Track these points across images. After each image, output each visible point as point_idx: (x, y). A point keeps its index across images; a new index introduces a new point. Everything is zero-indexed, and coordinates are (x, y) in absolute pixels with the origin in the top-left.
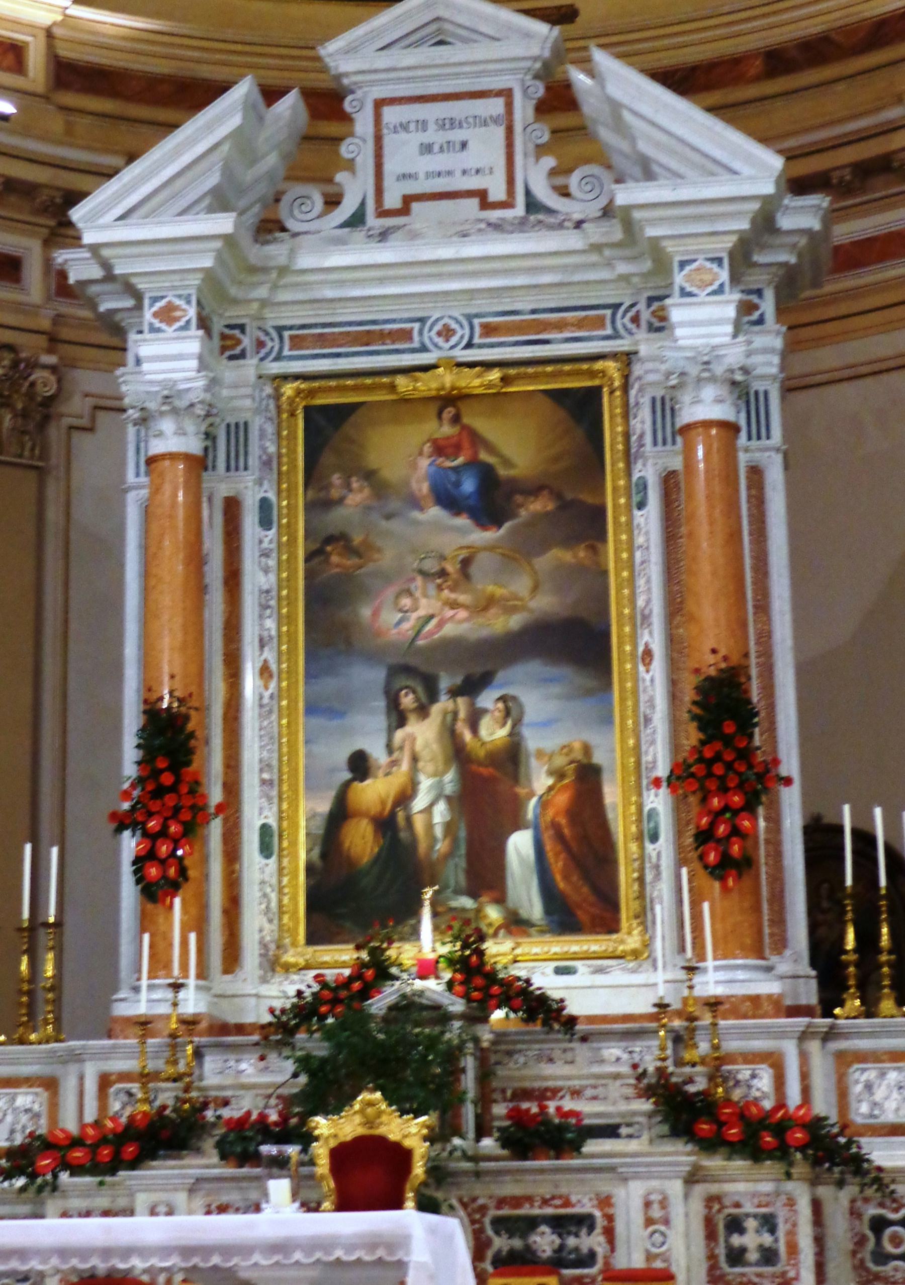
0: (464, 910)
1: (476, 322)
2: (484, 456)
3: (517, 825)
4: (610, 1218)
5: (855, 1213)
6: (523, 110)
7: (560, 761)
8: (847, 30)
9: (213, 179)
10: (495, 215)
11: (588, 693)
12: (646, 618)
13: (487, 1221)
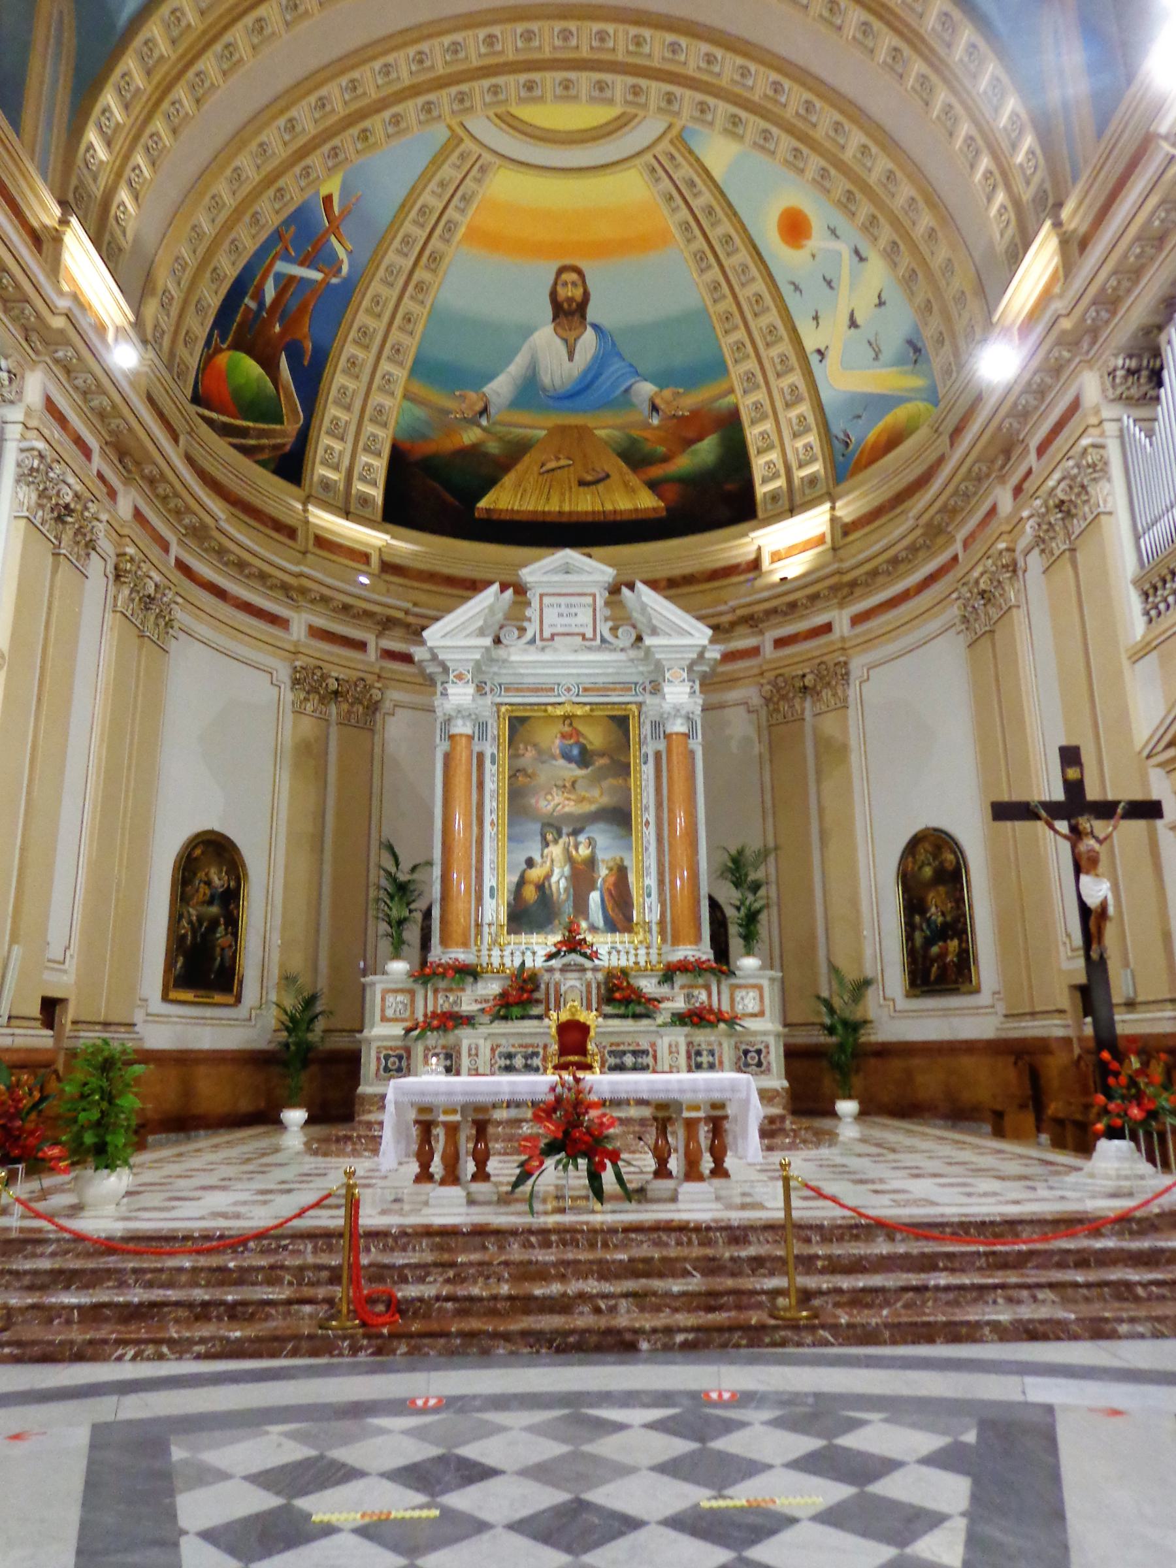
3: (593, 887)
5: (737, 1048)
6: (600, 602)
7: (611, 864)
8: (703, 573)
9: (480, 623)
10: (587, 643)
11: (622, 837)
12: (647, 808)
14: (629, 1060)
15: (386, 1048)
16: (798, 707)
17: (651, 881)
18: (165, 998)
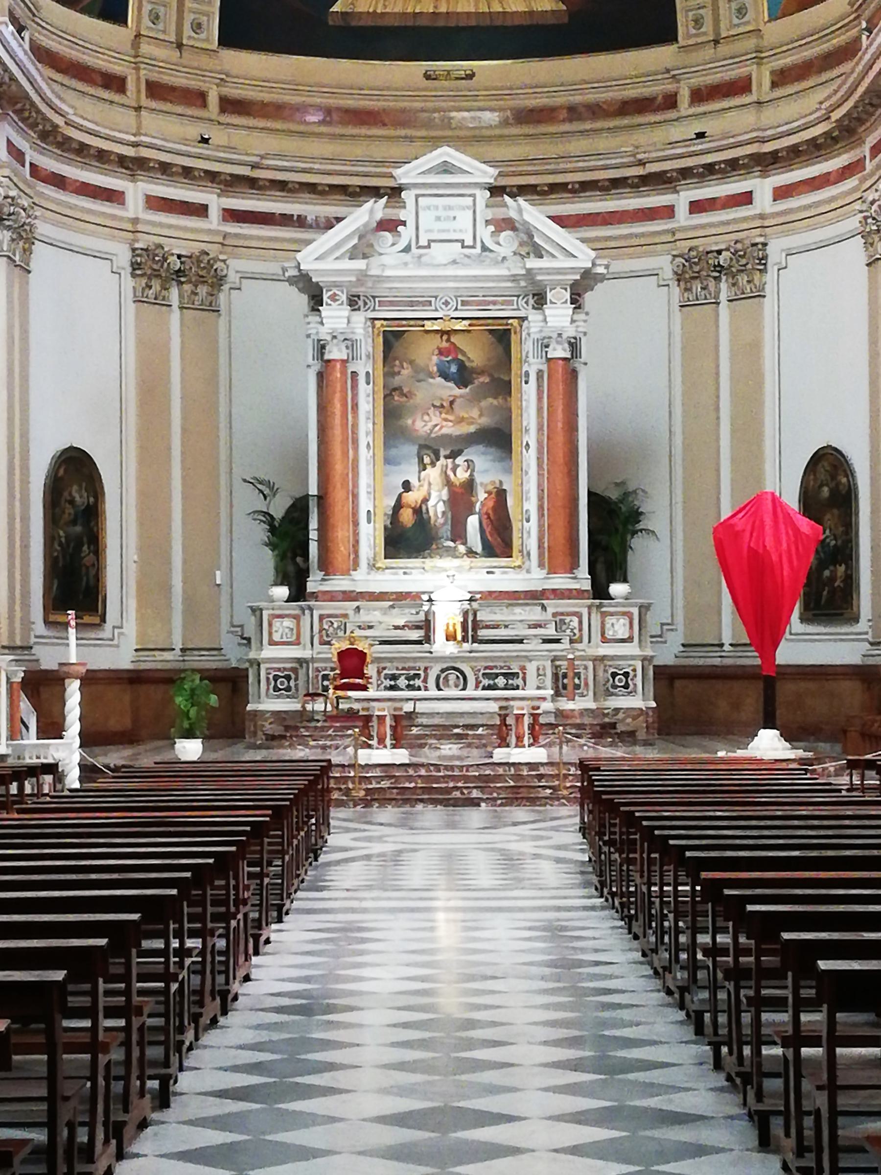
1: (459, 299)
2: (460, 357)
4: (524, 674)
5: (606, 671)
7: (490, 488)
11: (501, 460)
12: (527, 431)
13: (480, 674)
14: (501, 681)
17: (531, 505)
18: (47, 622)
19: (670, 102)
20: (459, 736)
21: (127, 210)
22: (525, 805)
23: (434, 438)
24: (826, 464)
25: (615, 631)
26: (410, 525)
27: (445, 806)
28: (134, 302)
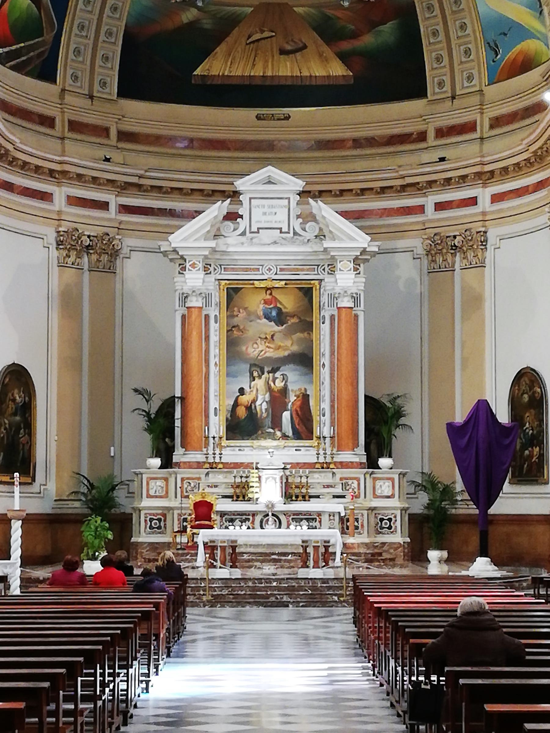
0: (270, 432)
2: (279, 305)
4: (321, 519)
5: (376, 517)
6: (293, 204)
7: (298, 393)
11: (306, 374)
13: (290, 519)
15: (150, 514)
16: (450, 260)
17: (326, 405)
19: (422, 137)
20: (275, 561)
21: (54, 205)
22: (318, 607)
23: (261, 359)
24: (526, 379)
25: (382, 491)
26: (243, 418)
27: (265, 607)
28: (58, 266)
